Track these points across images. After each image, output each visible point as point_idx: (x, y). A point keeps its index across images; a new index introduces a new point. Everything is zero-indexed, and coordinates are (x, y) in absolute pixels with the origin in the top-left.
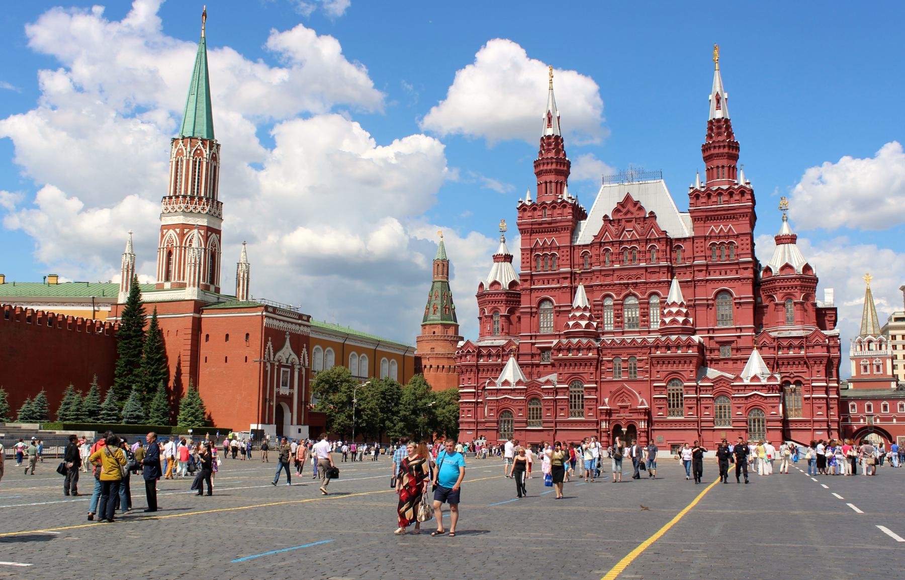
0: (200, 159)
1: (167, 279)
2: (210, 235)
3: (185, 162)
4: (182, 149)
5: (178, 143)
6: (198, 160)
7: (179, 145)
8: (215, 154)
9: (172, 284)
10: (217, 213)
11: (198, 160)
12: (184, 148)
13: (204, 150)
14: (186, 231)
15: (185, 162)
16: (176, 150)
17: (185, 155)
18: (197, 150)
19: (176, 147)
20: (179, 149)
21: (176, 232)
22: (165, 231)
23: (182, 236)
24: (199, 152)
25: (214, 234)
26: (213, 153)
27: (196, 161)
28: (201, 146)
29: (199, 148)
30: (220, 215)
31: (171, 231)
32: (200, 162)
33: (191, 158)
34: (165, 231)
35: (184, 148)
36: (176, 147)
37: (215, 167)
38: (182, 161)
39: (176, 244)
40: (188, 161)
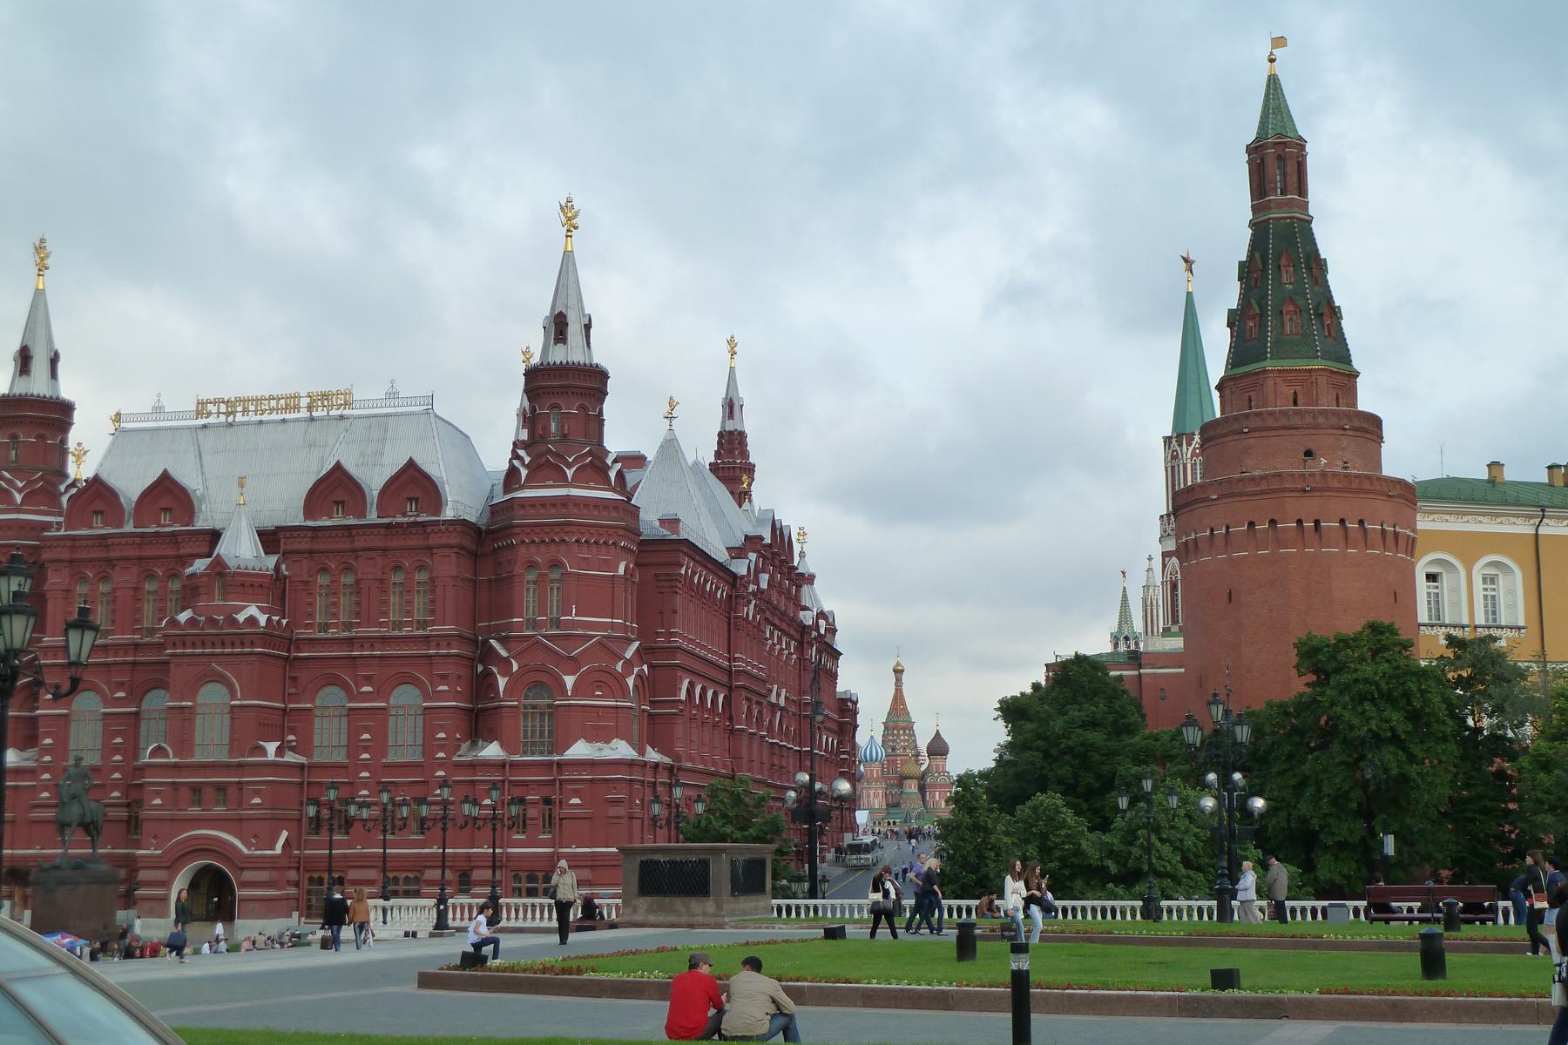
1: (1175, 621)
3: (1181, 466)
4: (1176, 451)
7: (1172, 446)
12: (1178, 449)
15: (1181, 466)
16: (1171, 451)
17: (1180, 456)
20: (1173, 452)
22: (1167, 559)
27: (1195, 464)
33: (1189, 461)
34: (1167, 559)
35: (1178, 449)
36: (1169, 447)
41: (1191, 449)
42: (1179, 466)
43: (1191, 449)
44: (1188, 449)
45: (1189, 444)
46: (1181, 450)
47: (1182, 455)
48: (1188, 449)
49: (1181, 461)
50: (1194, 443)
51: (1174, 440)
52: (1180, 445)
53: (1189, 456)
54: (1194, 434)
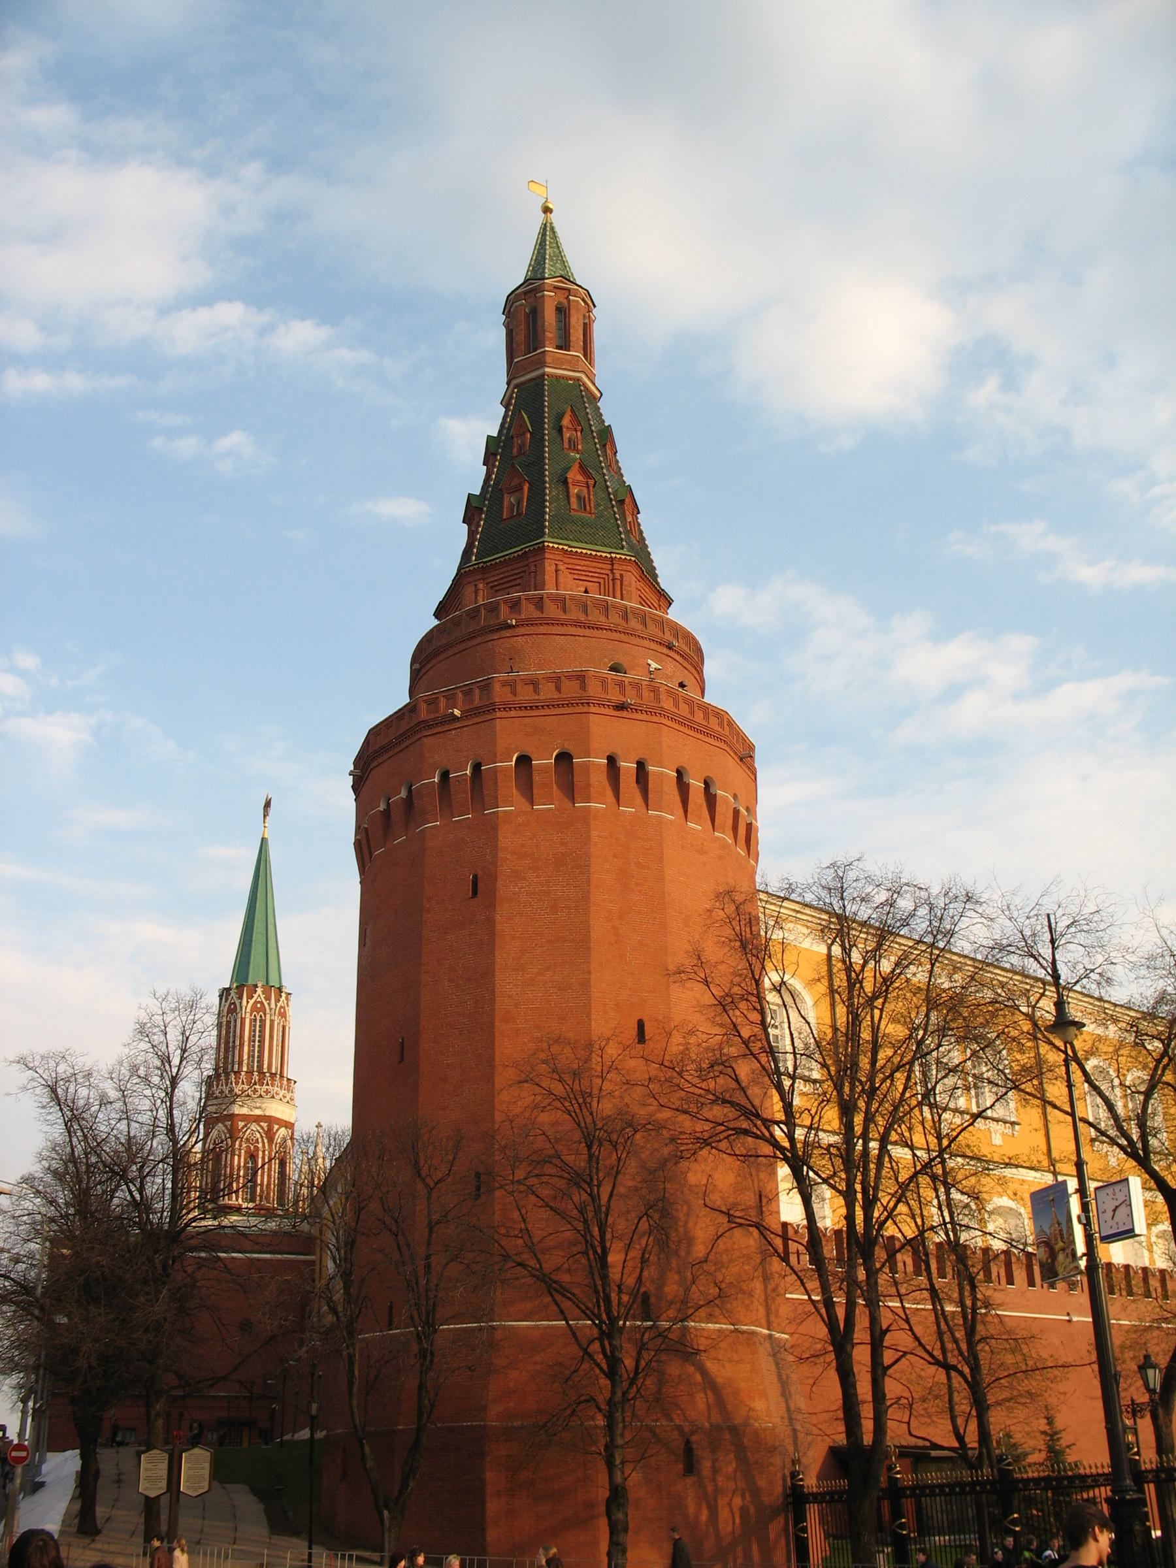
2: (277, 1130)
3: (239, 1021)
6: (258, 1018)
8: (284, 1008)
10: (288, 1098)
11: (258, 1018)
12: (237, 1002)
18: (256, 1002)
24: (259, 1005)
25: (283, 1129)
26: (281, 1007)
27: (255, 1020)
28: (262, 996)
30: (292, 1099)
32: (261, 1021)
33: (248, 1015)
37: (284, 1027)
40: (243, 1020)
41: (251, 1002)
42: (235, 1021)
43: (251, 1002)
44: (248, 1002)
45: (250, 997)
46: (241, 1003)
47: (241, 1008)
48: (248, 1002)
49: (239, 1015)
50: (256, 996)
51: (232, 992)
52: (241, 998)
53: (249, 1010)
54: (256, 986)
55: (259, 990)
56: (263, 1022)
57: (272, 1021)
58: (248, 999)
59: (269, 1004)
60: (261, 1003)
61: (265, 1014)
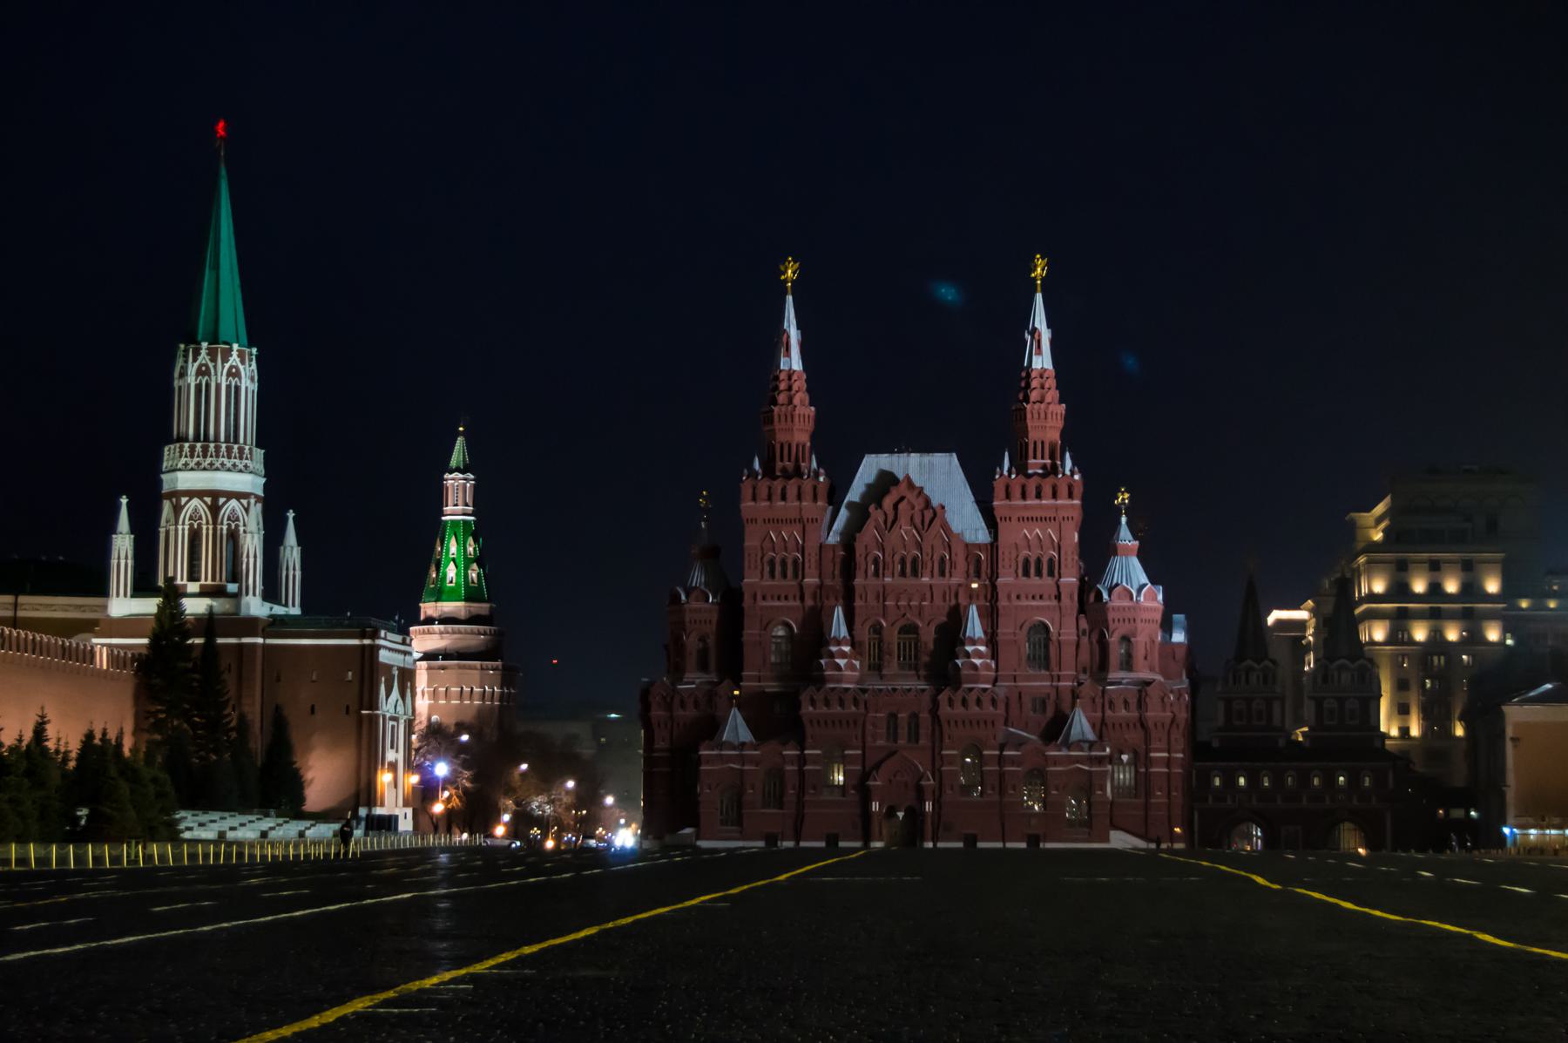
0: (236, 382)
4: (206, 365)
5: (200, 354)
6: (233, 384)
7: (200, 358)
9: (201, 586)
11: (233, 384)
12: (211, 365)
13: (241, 367)
14: (222, 500)
16: (196, 365)
18: (231, 367)
19: (195, 360)
21: (205, 503)
23: (215, 509)
29: (234, 364)
31: (195, 502)
35: (211, 365)
38: (208, 385)
39: (207, 523)
40: (218, 387)
41: (227, 366)
43: (227, 366)
45: (225, 360)
46: (215, 367)
48: (223, 367)
50: (231, 359)
52: (214, 360)
55: (235, 354)
56: (237, 389)
57: (247, 388)
58: (223, 363)
59: (245, 369)
60: (236, 367)
61: (241, 382)
